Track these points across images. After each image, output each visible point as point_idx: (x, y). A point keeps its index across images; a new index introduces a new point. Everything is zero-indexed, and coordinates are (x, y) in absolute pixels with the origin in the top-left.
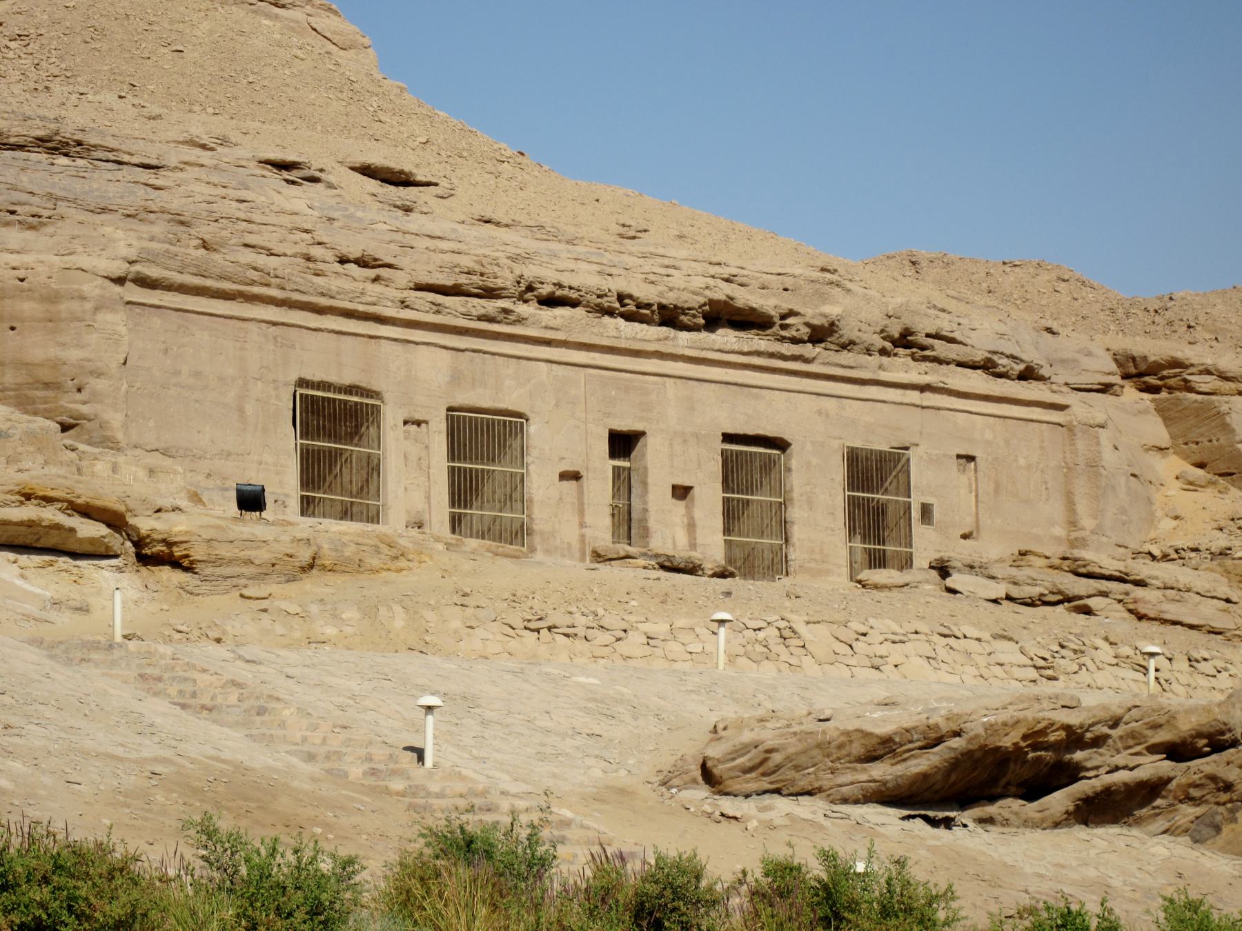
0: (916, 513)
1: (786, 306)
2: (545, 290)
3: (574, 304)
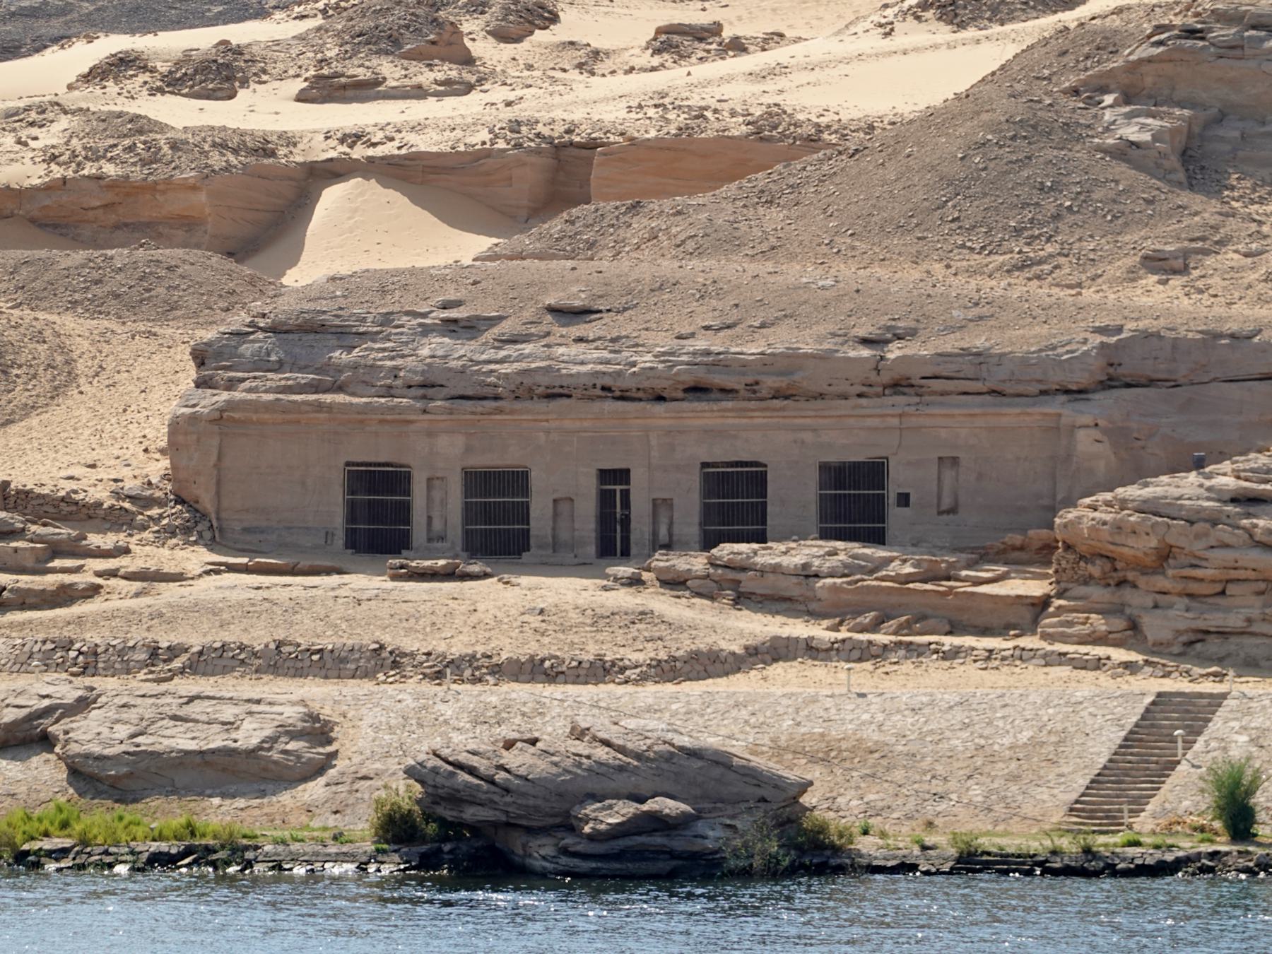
0: (892, 499)
1: (750, 379)
2: (540, 390)
3: (569, 396)
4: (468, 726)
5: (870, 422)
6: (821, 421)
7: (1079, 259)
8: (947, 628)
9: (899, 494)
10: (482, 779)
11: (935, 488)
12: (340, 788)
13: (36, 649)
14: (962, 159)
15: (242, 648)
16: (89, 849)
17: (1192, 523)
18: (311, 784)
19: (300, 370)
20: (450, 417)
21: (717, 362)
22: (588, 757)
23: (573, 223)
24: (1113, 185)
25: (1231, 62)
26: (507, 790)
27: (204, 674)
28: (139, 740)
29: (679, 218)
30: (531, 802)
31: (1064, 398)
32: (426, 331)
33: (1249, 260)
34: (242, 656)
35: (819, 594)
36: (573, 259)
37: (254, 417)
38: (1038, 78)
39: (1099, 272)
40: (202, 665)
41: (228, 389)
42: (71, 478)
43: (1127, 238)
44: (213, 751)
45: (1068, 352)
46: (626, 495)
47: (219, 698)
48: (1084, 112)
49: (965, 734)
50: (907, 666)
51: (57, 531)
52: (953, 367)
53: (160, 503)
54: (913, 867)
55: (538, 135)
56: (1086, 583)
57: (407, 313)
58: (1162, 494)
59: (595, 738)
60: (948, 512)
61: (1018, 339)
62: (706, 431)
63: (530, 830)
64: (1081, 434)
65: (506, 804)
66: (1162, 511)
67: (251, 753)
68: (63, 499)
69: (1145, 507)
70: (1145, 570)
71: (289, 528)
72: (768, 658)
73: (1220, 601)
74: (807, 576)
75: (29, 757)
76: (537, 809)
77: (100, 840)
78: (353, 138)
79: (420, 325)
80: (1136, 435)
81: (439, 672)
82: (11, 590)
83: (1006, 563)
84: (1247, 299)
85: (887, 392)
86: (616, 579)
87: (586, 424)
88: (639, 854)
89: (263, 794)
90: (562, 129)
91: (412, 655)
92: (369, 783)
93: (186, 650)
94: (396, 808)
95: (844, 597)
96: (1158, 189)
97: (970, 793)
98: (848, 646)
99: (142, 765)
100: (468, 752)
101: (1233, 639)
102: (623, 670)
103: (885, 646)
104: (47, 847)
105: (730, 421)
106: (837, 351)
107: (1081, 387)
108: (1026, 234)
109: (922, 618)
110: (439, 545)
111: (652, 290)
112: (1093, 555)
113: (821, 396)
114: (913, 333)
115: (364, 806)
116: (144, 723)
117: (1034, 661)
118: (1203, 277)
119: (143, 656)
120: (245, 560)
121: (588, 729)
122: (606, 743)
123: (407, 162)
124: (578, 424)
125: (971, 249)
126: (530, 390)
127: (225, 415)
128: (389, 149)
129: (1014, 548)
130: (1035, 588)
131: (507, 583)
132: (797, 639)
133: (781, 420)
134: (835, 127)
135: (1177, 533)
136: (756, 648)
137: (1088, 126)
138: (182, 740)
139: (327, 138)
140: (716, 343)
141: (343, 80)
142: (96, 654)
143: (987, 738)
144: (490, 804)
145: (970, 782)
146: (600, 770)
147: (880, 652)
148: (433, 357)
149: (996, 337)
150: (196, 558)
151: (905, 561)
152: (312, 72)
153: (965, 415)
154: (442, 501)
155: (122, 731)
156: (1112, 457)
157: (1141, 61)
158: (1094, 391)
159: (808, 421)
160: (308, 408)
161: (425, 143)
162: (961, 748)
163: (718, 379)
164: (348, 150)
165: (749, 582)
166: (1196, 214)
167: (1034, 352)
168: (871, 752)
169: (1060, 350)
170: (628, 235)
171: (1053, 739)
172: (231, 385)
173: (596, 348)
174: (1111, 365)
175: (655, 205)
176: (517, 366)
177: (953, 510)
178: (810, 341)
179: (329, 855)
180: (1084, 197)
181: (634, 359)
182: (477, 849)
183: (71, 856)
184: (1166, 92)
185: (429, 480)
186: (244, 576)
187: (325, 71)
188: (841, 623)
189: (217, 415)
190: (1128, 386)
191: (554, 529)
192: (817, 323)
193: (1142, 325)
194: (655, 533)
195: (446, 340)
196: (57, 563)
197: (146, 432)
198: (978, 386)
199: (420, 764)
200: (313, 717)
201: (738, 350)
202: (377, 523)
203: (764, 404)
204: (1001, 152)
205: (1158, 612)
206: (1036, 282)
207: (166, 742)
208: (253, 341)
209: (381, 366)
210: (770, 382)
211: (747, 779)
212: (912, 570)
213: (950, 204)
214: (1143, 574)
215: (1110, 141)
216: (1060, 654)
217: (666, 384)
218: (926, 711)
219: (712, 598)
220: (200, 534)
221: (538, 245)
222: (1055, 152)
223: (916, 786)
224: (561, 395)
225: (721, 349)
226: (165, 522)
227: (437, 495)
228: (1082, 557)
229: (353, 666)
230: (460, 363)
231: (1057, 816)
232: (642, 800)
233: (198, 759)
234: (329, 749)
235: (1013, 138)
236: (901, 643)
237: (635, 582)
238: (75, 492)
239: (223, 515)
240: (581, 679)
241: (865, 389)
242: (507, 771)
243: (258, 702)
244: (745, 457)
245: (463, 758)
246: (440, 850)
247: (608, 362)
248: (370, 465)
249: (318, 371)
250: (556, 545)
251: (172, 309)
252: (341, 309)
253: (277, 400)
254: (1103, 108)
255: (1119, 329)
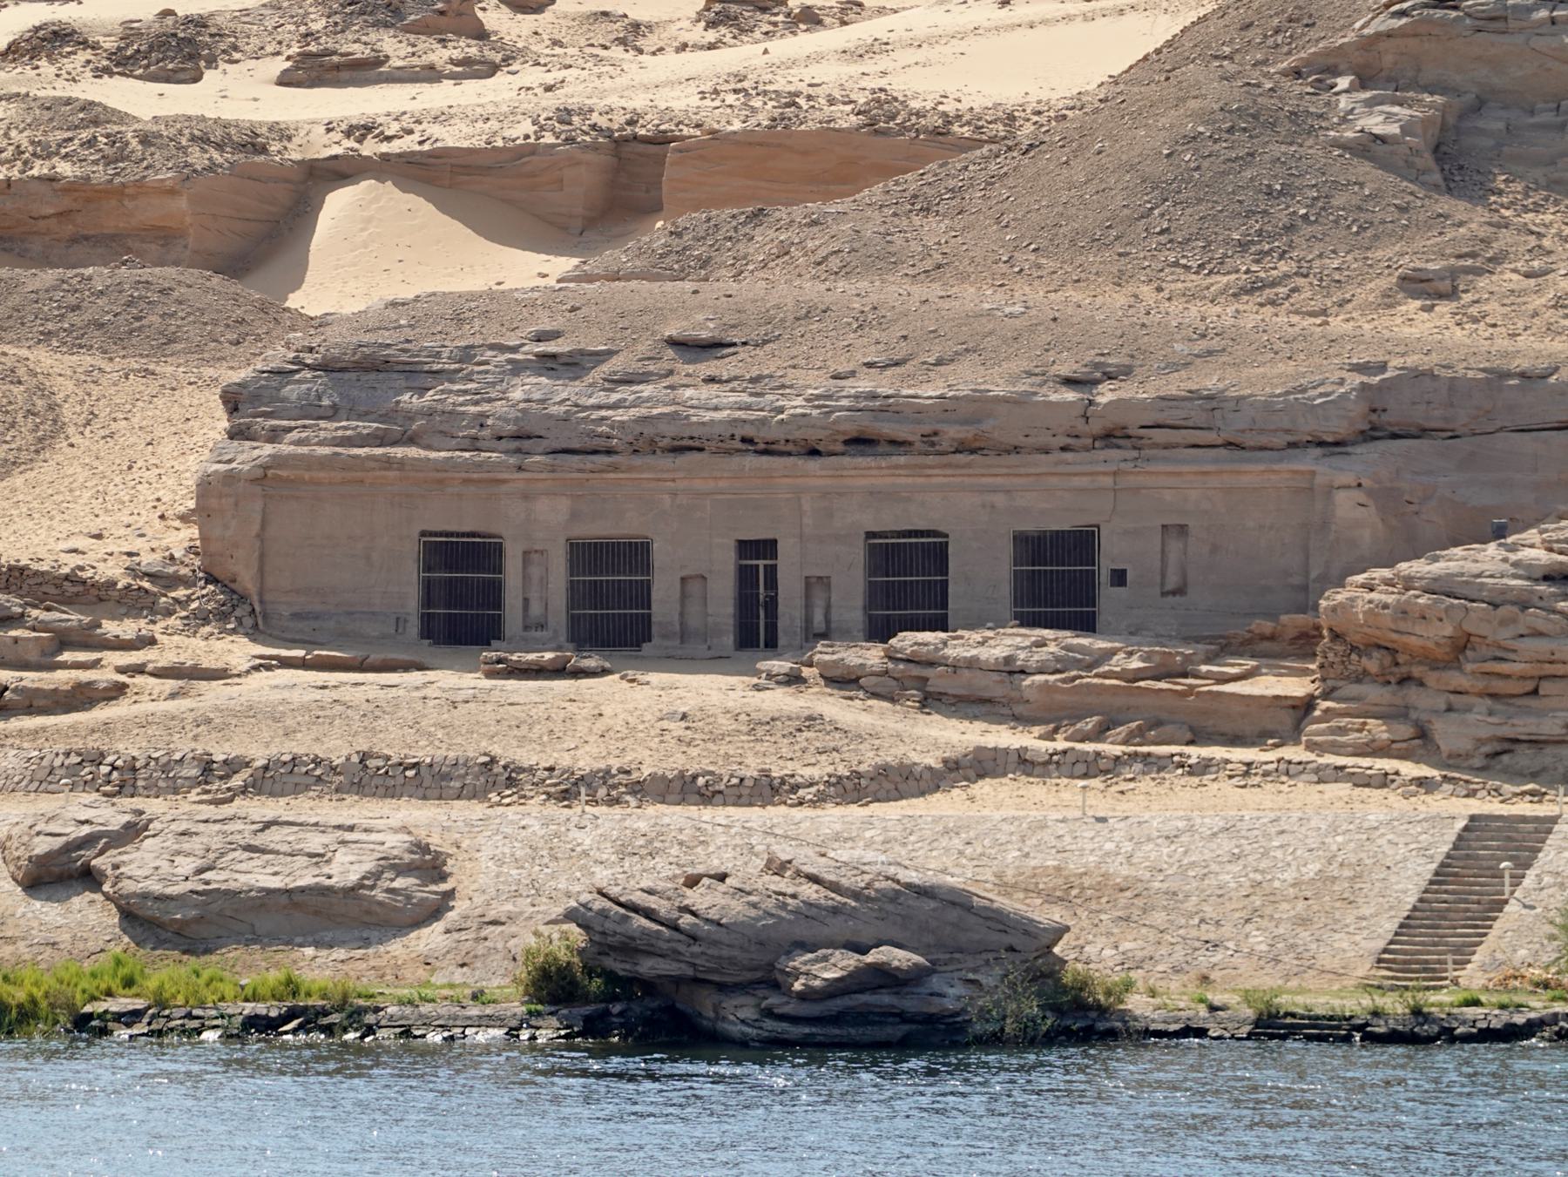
0: (1105, 576)
1: (927, 429)
2: (665, 442)
3: (701, 450)
4: (613, 858)
5: (1077, 482)
6: (1016, 480)
7: (1321, 280)
8: (1189, 736)
9: (1114, 571)
10: (662, 924)
11: (1158, 564)
12: (463, 936)
13: (57, 762)
14: (1168, 156)
15: (317, 762)
16: (167, 1012)
17: (1496, 606)
18: (425, 931)
19: (360, 417)
20: (552, 475)
21: (886, 407)
22: (794, 896)
23: (679, 235)
24: (1356, 188)
25: (1493, 37)
26: (694, 938)
27: (272, 794)
28: (208, 875)
29: (815, 229)
30: (725, 952)
31: (1318, 451)
32: (517, 368)
33: (1532, 282)
34: (318, 772)
35: (1027, 695)
36: (682, 279)
37: (307, 476)
38: (1216, 57)
39: (1348, 296)
40: (268, 784)
41: (271, 440)
42: (75, 551)
43: (1379, 254)
44: (302, 890)
45: (1321, 395)
46: (772, 572)
47: (301, 824)
48: (1314, 98)
49: (1236, 868)
50: (1146, 784)
51: (65, 616)
52: (1181, 414)
53: (186, 582)
54: (1201, 1033)
55: (594, 127)
56: (1358, 681)
57: (492, 347)
58: (1456, 570)
59: (798, 873)
60: (1174, 593)
61: (1260, 380)
62: (871, 493)
63: (722, 987)
64: (1341, 497)
65: (693, 955)
66: (1458, 591)
67: (350, 892)
68: (67, 578)
69: (1436, 586)
70: (1435, 665)
71: (350, 614)
72: (971, 773)
73: (1533, 702)
74: (1011, 673)
75: (69, 898)
76: (732, 961)
77: (180, 1000)
78: (364, 130)
79: (509, 361)
80: (1407, 497)
81: (566, 791)
82: (15, 690)
83: (1253, 657)
84: (1534, 330)
85: (1097, 444)
86: (770, 676)
87: (722, 484)
88: (862, 1017)
89: (366, 943)
90: (623, 120)
91: (531, 770)
92: (500, 928)
93: (247, 765)
94: (552, 958)
95: (1058, 697)
96: (1412, 193)
97: (1251, 940)
98: (1070, 758)
99: (215, 907)
100: (642, 890)
101: (1549, 750)
102: (795, 788)
103: (1117, 758)
104: (114, 1009)
105: (903, 480)
106: (1035, 394)
107: (1339, 438)
108: (1253, 249)
109: (1158, 724)
110: (539, 634)
111: (798, 319)
112: (1367, 645)
113: (1016, 449)
114: (1126, 372)
115: (498, 957)
116: (212, 856)
117: (1304, 777)
118: (1477, 302)
119: (194, 772)
120: (300, 653)
121: (790, 862)
122: (814, 879)
123: (432, 160)
124: (711, 484)
125: (1186, 267)
126: (652, 442)
127: (270, 472)
128: (407, 144)
129: (1263, 638)
130: (1296, 687)
131: (633, 681)
132: (1006, 751)
133: (966, 480)
134: (967, 117)
135: (1478, 619)
136: (956, 763)
137: (1321, 116)
138: (259, 876)
139: (329, 130)
140: (884, 384)
141: (335, 59)
142: (134, 770)
143: (1263, 872)
144: (675, 955)
145: (1249, 927)
146: (809, 912)
147: (1111, 765)
148: (528, 401)
149: (1231, 376)
150: (239, 651)
151: (1130, 654)
152: (295, 49)
153: (1196, 473)
154: (542, 579)
155: (186, 865)
156: (1380, 526)
157: (1378, 36)
158: (1353, 444)
159: (999, 480)
160: (372, 464)
161: (452, 137)
162: (1233, 885)
163: (888, 429)
164: (356, 145)
165: (938, 679)
166: (1461, 224)
167: (1279, 395)
168: (1122, 890)
169: (1311, 393)
170: (751, 250)
171: (1347, 873)
172: (274, 436)
173: (732, 391)
174: (1374, 411)
175: (782, 213)
176: (634, 412)
177: (1180, 591)
178: (1001, 381)
179: (469, 1018)
180: (1322, 203)
181: (780, 403)
182: (653, 1011)
183: (146, 1020)
184: (1410, 74)
185: (525, 553)
186: (300, 672)
187: (313, 48)
188: (1056, 730)
189: (260, 472)
190: (1395, 436)
191: (682, 614)
192: (1007, 358)
193: (1411, 361)
194: (808, 620)
195: (543, 380)
196: (67, 656)
197: (160, 494)
198: (1210, 437)
199: (584, 906)
200: (421, 848)
201: (911, 392)
202: (460, 606)
203: (945, 459)
204: (1217, 147)
205: (1453, 715)
206: (1269, 309)
207: (243, 878)
208: (299, 382)
209: (464, 413)
210: (953, 432)
211: (989, 923)
212: (1142, 665)
213: (1156, 212)
214: (1434, 669)
215: (1349, 134)
216: (1336, 768)
217: (821, 434)
218: (1184, 839)
219: (892, 700)
220: (239, 620)
221: (638, 263)
222: (1283, 148)
223: (1181, 932)
224: (690, 449)
225: (891, 392)
226: (194, 605)
227: (535, 572)
228: (1353, 648)
229: (458, 784)
230: (563, 409)
231: (1363, 969)
232: (863, 950)
233: (284, 900)
234: (443, 887)
235: (1230, 130)
236: (1136, 754)
237: (793, 680)
238: (82, 568)
239: (268, 597)
240: (743, 800)
241: (1070, 441)
242: (694, 914)
243: (351, 828)
244: (921, 525)
245: (638, 898)
246: (607, 1013)
247: (748, 408)
248: (451, 534)
249: (383, 418)
250: (684, 635)
251: (170, 342)
252: (408, 341)
253: (336, 454)
254: (1337, 94)
255: (1383, 367)
